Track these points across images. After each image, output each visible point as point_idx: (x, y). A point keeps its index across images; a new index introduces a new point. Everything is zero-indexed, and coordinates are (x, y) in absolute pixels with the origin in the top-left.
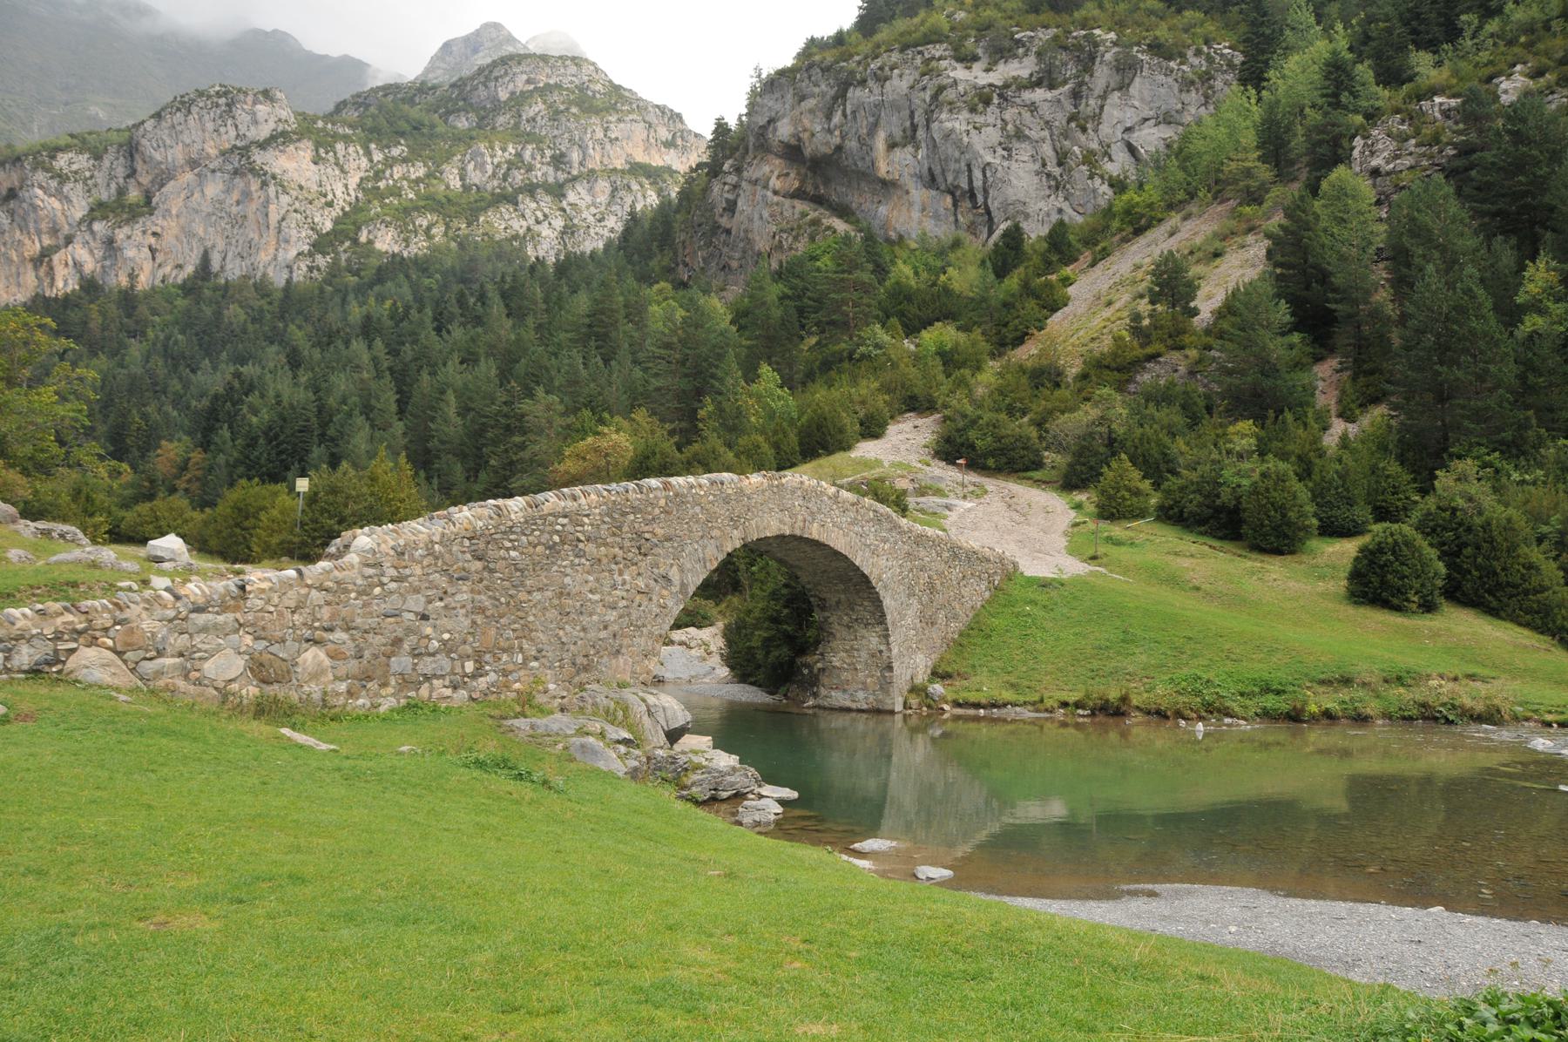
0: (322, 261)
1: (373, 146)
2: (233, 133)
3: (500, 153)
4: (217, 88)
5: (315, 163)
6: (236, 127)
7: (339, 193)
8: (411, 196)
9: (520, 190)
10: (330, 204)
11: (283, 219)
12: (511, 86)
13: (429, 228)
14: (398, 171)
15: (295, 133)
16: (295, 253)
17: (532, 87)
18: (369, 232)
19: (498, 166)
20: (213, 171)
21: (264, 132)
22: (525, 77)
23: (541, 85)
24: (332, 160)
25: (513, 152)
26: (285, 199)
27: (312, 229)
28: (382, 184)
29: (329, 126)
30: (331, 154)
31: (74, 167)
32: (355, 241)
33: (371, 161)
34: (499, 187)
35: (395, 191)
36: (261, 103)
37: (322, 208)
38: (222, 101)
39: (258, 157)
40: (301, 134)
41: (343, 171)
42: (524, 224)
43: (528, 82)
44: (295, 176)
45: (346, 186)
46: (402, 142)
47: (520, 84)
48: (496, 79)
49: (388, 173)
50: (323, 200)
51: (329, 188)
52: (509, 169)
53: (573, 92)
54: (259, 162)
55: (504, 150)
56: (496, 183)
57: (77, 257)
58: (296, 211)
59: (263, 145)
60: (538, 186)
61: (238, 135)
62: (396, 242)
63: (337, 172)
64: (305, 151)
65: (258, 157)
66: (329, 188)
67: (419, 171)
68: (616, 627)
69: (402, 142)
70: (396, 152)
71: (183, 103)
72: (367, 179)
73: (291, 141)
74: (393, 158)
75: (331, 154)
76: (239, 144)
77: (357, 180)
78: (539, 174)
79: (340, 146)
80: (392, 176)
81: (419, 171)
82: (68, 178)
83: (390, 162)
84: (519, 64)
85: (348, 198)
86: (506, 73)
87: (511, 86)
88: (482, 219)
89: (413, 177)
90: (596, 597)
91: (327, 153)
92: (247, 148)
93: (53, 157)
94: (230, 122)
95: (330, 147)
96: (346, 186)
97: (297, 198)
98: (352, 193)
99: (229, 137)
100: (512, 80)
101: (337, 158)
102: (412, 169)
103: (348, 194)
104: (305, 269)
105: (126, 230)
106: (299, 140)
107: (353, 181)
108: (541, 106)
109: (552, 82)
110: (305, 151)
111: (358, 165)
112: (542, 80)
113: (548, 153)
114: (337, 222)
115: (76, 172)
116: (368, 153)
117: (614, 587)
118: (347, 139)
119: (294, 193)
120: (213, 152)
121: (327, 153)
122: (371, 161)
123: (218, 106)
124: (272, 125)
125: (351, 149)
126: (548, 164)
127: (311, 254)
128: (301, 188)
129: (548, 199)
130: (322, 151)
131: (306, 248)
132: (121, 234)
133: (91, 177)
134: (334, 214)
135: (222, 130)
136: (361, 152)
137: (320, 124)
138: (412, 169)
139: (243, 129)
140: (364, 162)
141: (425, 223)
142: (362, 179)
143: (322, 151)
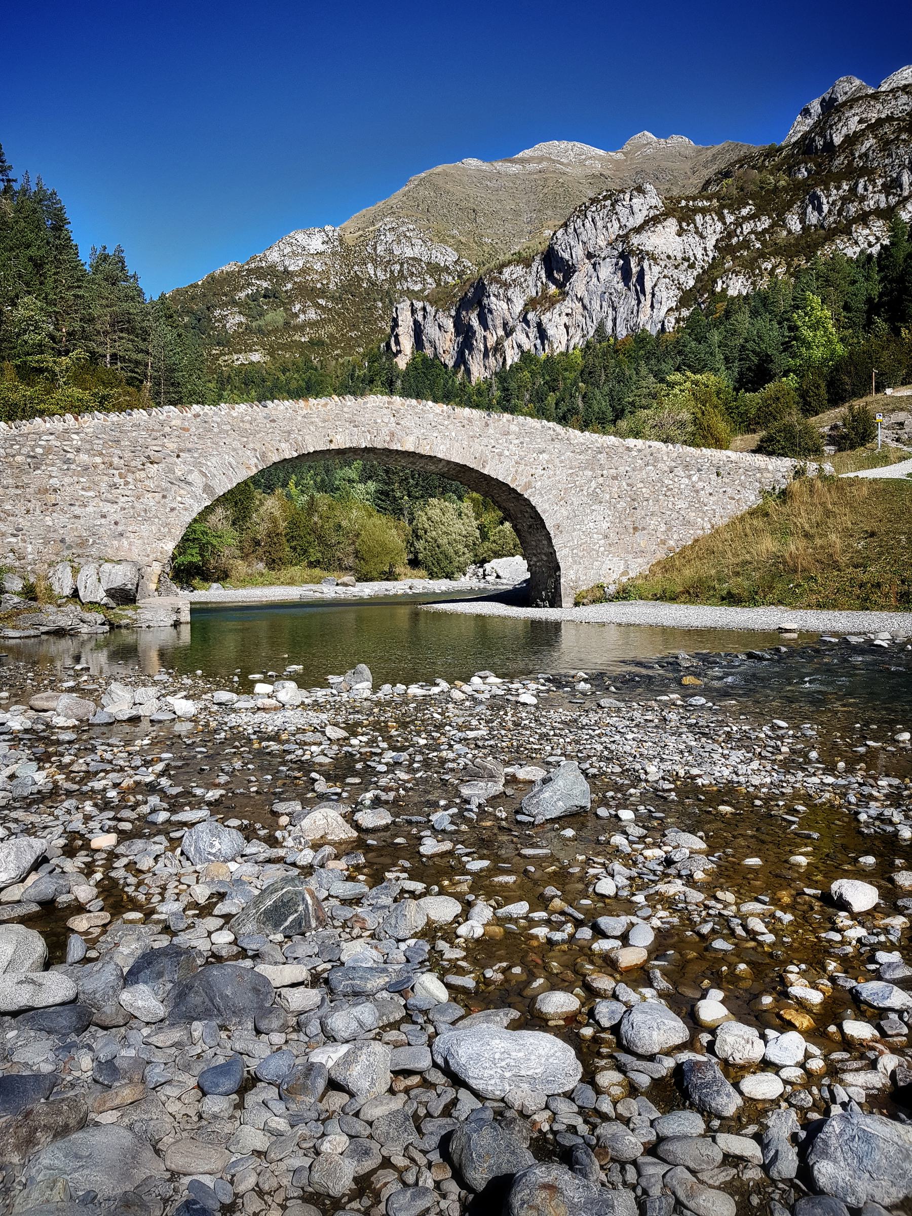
0: (685, 313)
1: (726, 211)
2: (616, 225)
3: (835, 192)
4: (605, 194)
5: (680, 235)
6: (619, 220)
7: (699, 256)
8: (758, 245)
9: (855, 220)
10: (692, 266)
11: (655, 285)
12: (845, 130)
13: (774, 268)
14: (747, 227)
15: (661, 215)
16: (666, 310)
17: (864, 126)
18: (723, 282)
19: (834, 203)
20: (604, 259)
21: (639, 220)
22: (857, 118)
23: (873, 121)
24: (693, 230)
25: (847, 188)
26: (656, 269)
27: (678, 289)
28: (734, 241)
29: (691, 203)
30: (692, 225)
31: (514, 277)
32: (713, 293)
33: (725, 223)
34: (835, 222)
35: (746, 244)
36: (636, 197)
37: (686, 270)
38: (608, 202)
39: (635, 240)
40: (666, 215)
41: (702, 237)
42: (858, 250)
43: (860, 122)
44: (664, 249)
45: (705, 249)
46: (750, 202)
47: (854, 125)
48: (831, 127)
49: (738, 231)
50: (686, 264)
51: (691, 253)
52: (843, 204)
53: (904, 120)
54: (636, 244)
55: (838, 188)
56: (831, 219)
57: (519, 341)
58: (665, 277)
59: (638, 230)
60: (870, 213)
61: (621, 227)
62: (745, 286)
63: (697, 239)
64: (672, 224)
65: (635, 240)
66: (691, 253)
67: (765, 223)
68: (117, 517)
69: (750, 202)
70: (744, 212)
71: (580, 211)
72: (722, 239)
73: (660, 222)
74: (743, 217)
75: (692, 225)
76: (621, 233)
77: (714, 242)
78: (872, 203)
79: (699, 218)
80: (742, 232)
81: (765, 223)
82: (510, 285)
83: (739, 223)
84: (851, 108)
85: (706, 258)
86: (840, 120)
87: (845, 130)
88: (819, 253)
89: (760, 230)
90: (91, 494)
91: (688, 225)
92: (626, 236)
93: (500, 273)
94: (614, 217)
95: (690, 220)
96: (705, 249)
97: (666, 266)
98: (711, 254)
99: (615, 229)
100: (846, 125)
101: (696, 228)
102: (758, 223)
103: (707, 255)
104: (673, 321)
105: (548, 314)
106: (665, 220)
107: (711, 243)
108: (872, 141)
109: (883, 116)
110: (672, 224)
111: (713, 230)
112: (873, 116)
113: (879, 182)
114: (698, 279)
115: (514, 280)
116: (722, 219)
117: (115, 486)
118: (704, 211)
119: (662, 263)
120: (603, 244)
121: (688, 225)
122: (725, 223)
123: (605, 206)
124: (645, 213)
125: (708, 217)
126: (880, 192)
127: (677, 309)
128: (669, 257)
129: (880, 223)
130: (684, 224)
131: (674, 305)
132: (545, 319)
133: (525, 280)
134: (695, 273)
135: (609, 225)
136: (716, 218)
137: (683, 203)
138: (758, 223)
139: (623, 221)
140: (719, 226)
141: (770, 267)
142: (717, 240)
143: (684, 224)
